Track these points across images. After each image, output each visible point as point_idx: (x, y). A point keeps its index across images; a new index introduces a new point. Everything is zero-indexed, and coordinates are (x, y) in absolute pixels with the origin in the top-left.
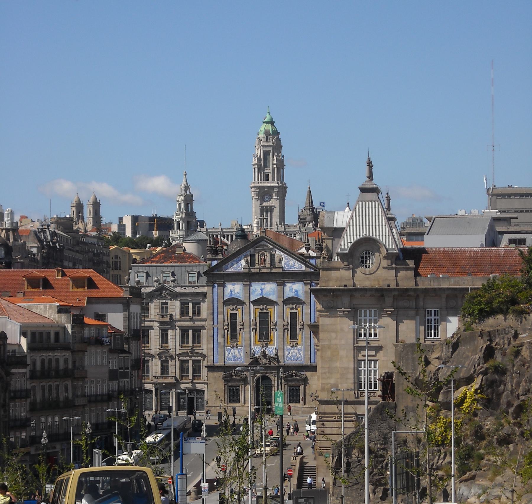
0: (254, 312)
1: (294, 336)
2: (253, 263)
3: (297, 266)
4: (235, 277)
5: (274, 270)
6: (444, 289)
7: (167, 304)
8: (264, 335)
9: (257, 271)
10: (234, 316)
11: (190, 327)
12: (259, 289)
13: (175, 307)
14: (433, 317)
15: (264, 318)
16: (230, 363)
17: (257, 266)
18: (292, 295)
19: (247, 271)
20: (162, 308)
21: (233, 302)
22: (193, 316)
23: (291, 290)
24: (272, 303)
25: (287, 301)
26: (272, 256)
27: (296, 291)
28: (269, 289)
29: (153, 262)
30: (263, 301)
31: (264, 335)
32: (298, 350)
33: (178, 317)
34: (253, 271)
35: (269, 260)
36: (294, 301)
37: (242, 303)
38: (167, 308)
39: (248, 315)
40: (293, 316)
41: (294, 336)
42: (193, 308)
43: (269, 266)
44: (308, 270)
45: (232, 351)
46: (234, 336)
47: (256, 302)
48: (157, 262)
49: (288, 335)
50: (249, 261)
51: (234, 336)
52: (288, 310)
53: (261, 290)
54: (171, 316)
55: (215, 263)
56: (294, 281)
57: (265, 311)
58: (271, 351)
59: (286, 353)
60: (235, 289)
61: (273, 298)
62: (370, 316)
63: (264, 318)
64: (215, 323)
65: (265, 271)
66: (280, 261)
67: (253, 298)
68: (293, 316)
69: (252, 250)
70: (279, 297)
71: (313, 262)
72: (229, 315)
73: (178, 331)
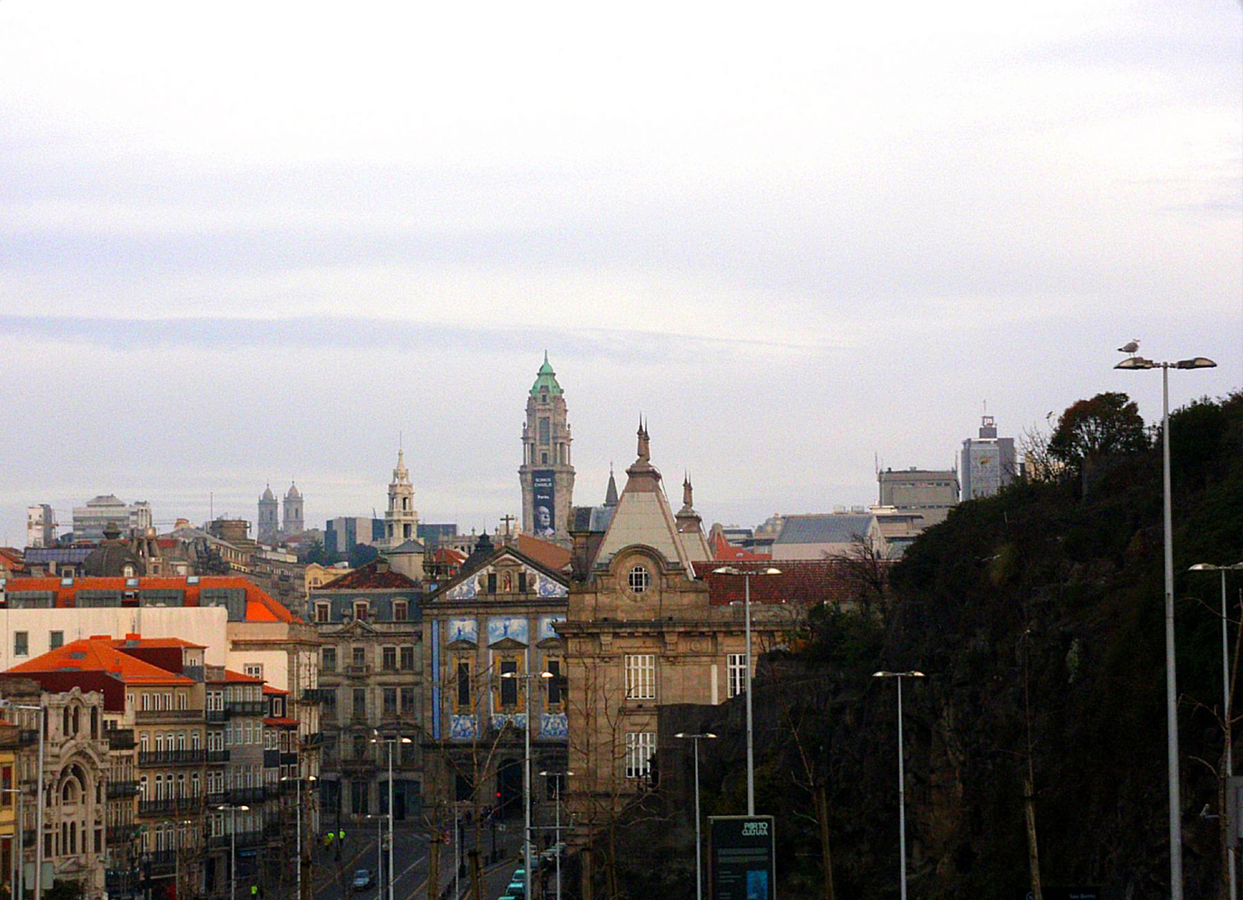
2: (492, 587)
4: (464, 607)
5: (522, 598)
7: (363, 650)
9: (498, 598)
10: (463, 669)
11: (399, 684)
13: (375, 655)
14: (738, 667)
16: (460, 739)
17: (498, 591)
19: (480, 598)
20: (355, 657)
21: (464, 645)
22: (403, 668)
24: (520, 646)
26: (522, 576)
28: (517, 626)
29: (341, 587)
30: (509, 645)
32: (562, 718)
33: (378, 670)
34: (491, 598)
35: (516, 581)
37: (474, 647)
38: (362, 657)
42: (403, 656)
43: (517, 590)
45: (461, 722)
46: (464, 698)
47: (496, 646)
48: (348, 587)
50: (487, 584)
51: (464, 698)
53: (505, 628)
54: (368, 667)
55: (434, 587)
57: (510, 660)
59: (544, 724)
60: (463, 626)
61: (523, 640)
62: (644, 664)
64: (436, 680)
65: (509, 598)
66: (532, 585)
67: (491, 641)
69: (491, 569)
70: (531, 638)
72: (456, 667)
73: (379, 691)
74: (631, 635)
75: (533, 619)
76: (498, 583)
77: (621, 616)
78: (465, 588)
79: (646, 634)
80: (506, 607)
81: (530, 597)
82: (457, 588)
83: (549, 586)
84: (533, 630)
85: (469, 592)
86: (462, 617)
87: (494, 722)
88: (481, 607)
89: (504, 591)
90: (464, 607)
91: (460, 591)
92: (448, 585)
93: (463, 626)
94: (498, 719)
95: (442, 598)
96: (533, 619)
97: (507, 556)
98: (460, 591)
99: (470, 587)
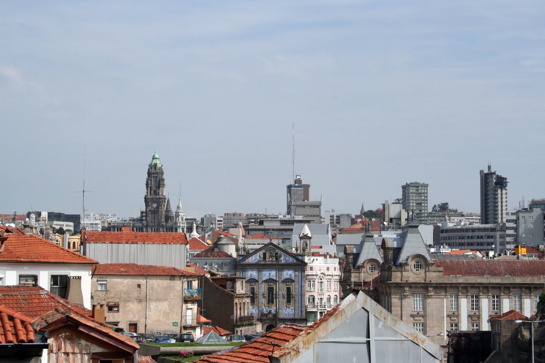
1: (289, 301)
2: (265, 258)
3: (291, 260)
4: (252, 266)
6: (461, 284)
8: (271, 301)
17: (267, 260)
18: (288, 277)
21: (252, 281)
23: (287, 274)
24: (275, 281)
26: (277, 254)
27: (290, 275)
28: (273, 274)
30: (269, 281)
37: (257, 281)
39: (262, 289)
40: (289, 289)
41: (289, 301)
44: (298, 263)
47: (266, 281)
49: (285, 301)
53: (270, 274)
56: (289, 269)
60: (252, 274)
63: (271, 290)
67: (264, 279)
68: (289, 289)
71: (300, 258)
74: (416, 287)
76: (267, 257)
77: (411, 280)
78: (254, 258)
79: (421, 287)
81: (280, 263)
82: (251, 258)
83: (287, 258)
85: (255, 260)
86: (252, 269)
87: (264, 310)
90: (252, 266)
91: (252, 260)
95: (244, 262)
97: (271, 246)
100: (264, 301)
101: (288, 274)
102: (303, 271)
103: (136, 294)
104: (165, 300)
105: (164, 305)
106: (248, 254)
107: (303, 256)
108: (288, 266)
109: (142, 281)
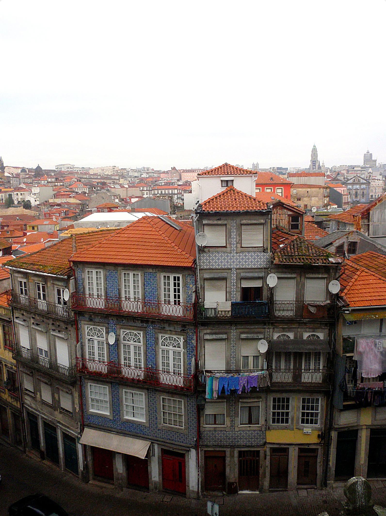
0: (354, 192)
1: (363, 197)
3: (364, 181)
8: (356, 197)
12: (355, 187)
15: (356, 193)
25: (362, 189)
31: (356, 197)
36: (364, 189)
40: (363, 192)
41: (363, 197)
52: (362, 191)
58: (358, 200)
60: (350, 187)
63: (356, 193)
68: (363, 192)
75: (360, 185)
80: (356, 184)
84: (360, 187)
88: (353, 184)
89: (356, 182)
92: (348, 181)
93: (350, 187)
94: (355, 200)
96: (360, 185)
98: (349, 182)
99: (351, 181)
100: (354, 197)
101: (363, 186)
102: (369, 185)
103: (307, 195)
104: (317, 197)
105: (317, 199)
106: (348, 180)
107: (369, 180)
108: (363, 184)
109: (309, 189)
